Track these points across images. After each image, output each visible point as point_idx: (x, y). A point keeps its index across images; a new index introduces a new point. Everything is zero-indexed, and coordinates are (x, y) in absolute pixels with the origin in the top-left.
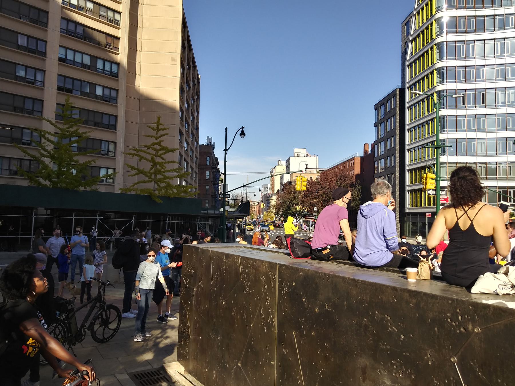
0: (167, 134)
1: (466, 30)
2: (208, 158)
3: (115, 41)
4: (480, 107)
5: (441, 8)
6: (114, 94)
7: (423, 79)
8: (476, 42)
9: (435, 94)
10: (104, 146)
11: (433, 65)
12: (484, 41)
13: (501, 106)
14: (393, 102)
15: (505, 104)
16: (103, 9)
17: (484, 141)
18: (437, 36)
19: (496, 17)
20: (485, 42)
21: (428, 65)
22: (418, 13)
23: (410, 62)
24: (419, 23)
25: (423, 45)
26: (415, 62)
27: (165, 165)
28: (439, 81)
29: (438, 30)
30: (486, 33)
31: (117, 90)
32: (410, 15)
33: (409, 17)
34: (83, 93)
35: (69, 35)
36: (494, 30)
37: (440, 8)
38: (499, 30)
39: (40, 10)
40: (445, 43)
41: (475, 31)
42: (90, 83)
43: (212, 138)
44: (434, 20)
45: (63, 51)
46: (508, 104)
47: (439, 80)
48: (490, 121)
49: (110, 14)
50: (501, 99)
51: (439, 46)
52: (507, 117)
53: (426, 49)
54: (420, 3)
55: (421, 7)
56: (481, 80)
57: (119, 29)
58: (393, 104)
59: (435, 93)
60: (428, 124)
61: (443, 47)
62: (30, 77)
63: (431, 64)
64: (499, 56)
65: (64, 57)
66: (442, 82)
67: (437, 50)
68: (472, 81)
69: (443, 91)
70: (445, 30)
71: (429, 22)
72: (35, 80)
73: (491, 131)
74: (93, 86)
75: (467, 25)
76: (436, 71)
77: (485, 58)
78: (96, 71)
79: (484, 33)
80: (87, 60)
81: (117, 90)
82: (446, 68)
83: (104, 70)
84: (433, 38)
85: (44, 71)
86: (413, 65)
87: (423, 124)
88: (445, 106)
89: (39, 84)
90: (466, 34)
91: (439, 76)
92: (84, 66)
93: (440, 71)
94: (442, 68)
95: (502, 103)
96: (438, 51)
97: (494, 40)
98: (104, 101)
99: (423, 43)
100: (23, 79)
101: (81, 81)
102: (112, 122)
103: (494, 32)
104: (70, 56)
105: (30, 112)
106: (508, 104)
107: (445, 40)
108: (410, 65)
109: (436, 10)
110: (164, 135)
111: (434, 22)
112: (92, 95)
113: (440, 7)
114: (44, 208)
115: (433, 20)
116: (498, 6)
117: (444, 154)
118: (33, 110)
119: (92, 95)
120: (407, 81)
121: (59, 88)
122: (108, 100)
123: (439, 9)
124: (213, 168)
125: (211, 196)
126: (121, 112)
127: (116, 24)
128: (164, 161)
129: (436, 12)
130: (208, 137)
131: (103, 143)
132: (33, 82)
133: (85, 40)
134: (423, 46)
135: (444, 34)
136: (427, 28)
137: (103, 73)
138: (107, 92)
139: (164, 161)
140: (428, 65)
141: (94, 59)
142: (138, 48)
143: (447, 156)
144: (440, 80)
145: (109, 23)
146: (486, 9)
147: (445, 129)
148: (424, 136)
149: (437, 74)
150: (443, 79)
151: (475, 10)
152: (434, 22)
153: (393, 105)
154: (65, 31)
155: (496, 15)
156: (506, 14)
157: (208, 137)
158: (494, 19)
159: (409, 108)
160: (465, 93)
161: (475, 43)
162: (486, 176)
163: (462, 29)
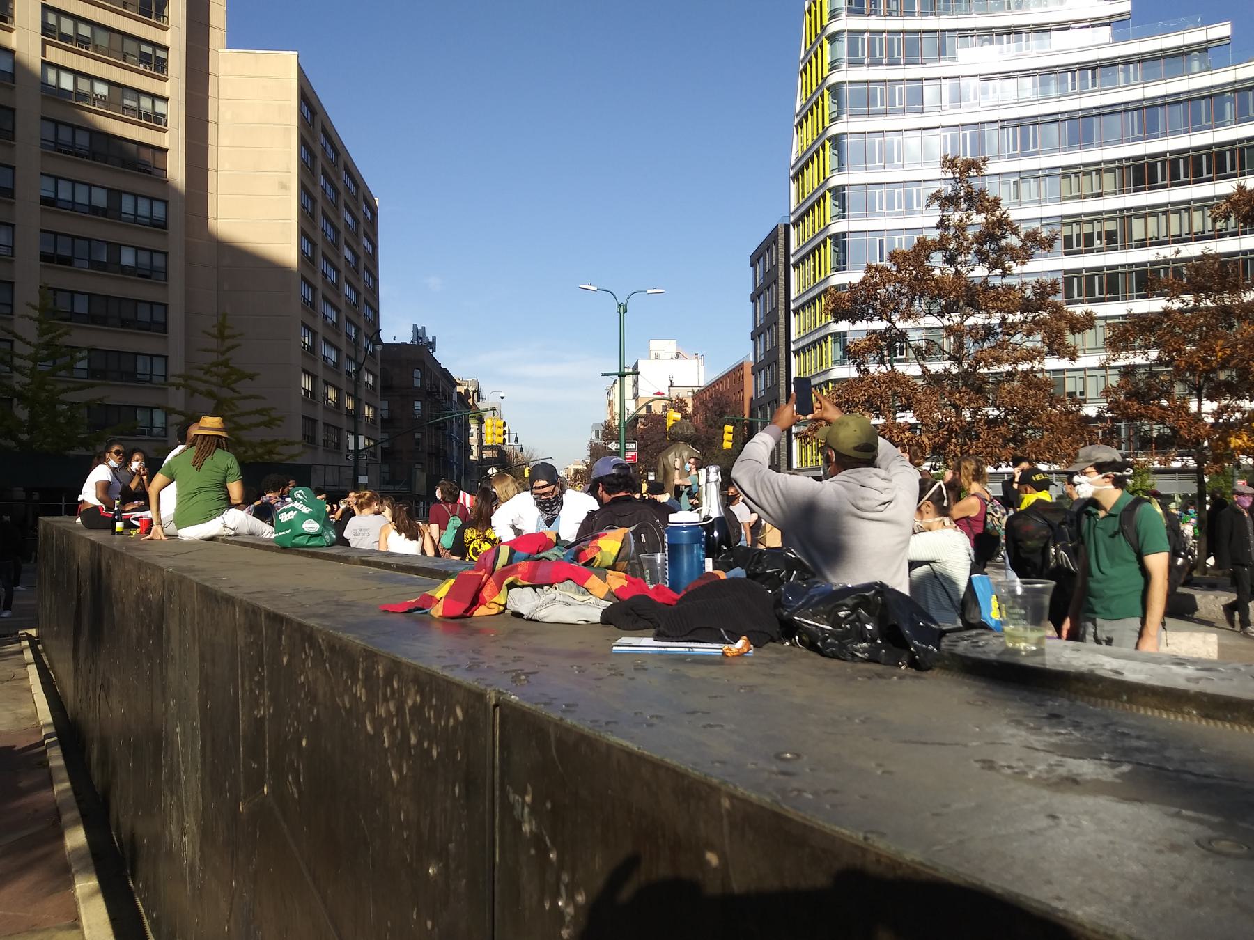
0: (239, 345)
2: (417, 373)
3: (158, 155)
6: (159, 261)
10: (142, 366)
16: (128, 93)
18: (832, 120)
22: (805, 69)
29: (835, 108)
31: (166, 254)
34: (94, 264)
35: (60, 151)
42: (108, 243)
43: (424, 328)
45: (49, 184)
47: (837, 210)
49: (146, 103)
57: (165, 131)
65: (52, 195)
68: (879, 215)
69: (844, 234)
74: (115, 248)
80: (100, 198)
81: (166, 254)
83: (136, 215)
85: (13, 226)
92: (95, 210)
94: (841, 188)
98: (140, 276)
101: (90, 240)
102: (158, 317)
104: (64, 193)
110: (233, 347)
111: (826, 93)
112: (112, 266)
114: (22, 489)
119: (112, 266)
121: (44, 257)
122: (148, 273)
124: (430, 394)
125: (428, 453)
126: (175, 294)
127: (158, 122)
128: (236, 395)
129: (830, 70)
130: (415, 326)
131: (140, 360)
133: (94, 159)
137: (136, 221)
138: (144, 258)
141: (115, 195)
145: (143, 121)
154: (52, 144)
157: (415, 326)
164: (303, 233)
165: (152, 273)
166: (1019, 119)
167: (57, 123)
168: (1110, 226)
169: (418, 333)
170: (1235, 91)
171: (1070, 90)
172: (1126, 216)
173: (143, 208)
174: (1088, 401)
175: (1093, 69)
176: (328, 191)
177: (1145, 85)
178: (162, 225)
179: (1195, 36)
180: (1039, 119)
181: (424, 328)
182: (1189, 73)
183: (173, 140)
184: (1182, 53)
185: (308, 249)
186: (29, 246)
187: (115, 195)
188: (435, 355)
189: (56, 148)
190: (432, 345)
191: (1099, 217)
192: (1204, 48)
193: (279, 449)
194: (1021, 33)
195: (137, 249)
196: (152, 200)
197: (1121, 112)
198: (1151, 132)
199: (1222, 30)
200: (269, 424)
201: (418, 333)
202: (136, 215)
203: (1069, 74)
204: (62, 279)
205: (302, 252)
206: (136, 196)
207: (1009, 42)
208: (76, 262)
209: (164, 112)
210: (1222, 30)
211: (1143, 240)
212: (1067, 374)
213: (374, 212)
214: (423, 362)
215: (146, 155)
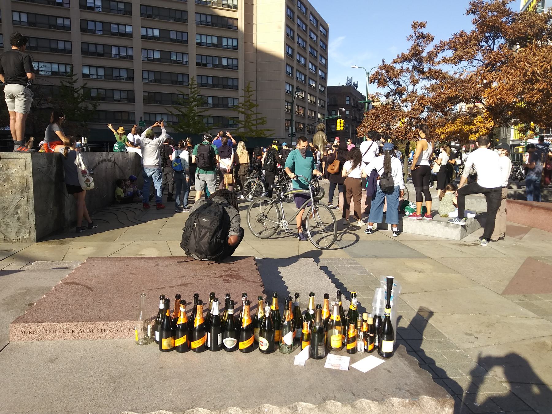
2: (348, 98)
3: (235, 21)
6: (235, 62)
27: (252, 115)
34: (214, 66)
35: (202, 24)
39: (182, 11)
42: (218, 57)
45: (198, 37)
57: (237, 11)
62: (180, 59)
65: (199, 41)
72: (183, 61)
74: (220, 59)
78: (222, 47)
80: (215, 41)
83: (227, 45)
85: (188, 54)
89: (185, 63)
92: (214, 45)
98: (229, 68)
100: (175, 62)
101: (212, 56)
102: (235, 84)
104: (204, 40)
105: (181, 83)
118: (183, 82)
121: (198, 64)
122: (232, 67)
124: (353, 107)
126: (241, 75)
128: (253, 113)
130: (348, 77)
131: (230, 100)
132: (182, 63)
133: (213, 26)
138: (230, 61)
139: (253, 113)
141: (220, 38)
142: (254, 22)
145: (229, 9)
154: (199, 22)
157: (348, 77)
164: (287, 45)
165: (233, 68)
167: (201, 14)
169: (349, 81)
173: (230, 43)
176: (301, 25)
178: (236, 48)
181: (352, 78)
183: (239, 15)
185: (290, 52)
186: (193, 60)
187: (220, 38)
188: (357, 89)
189: (201, 24)
190: (356, 85)
193: (265, 132)
195: (228, 58)
196: (233, 39)
200: (262, 123)
201: (349, 81)
202: (227, 45)
204: (204, 72)
205: (287, 54)
206: (227, 38)
208: (208, 65)
209: (236, 4)
213: (327, 31)
214: (351, 93)
215: (230, 21)
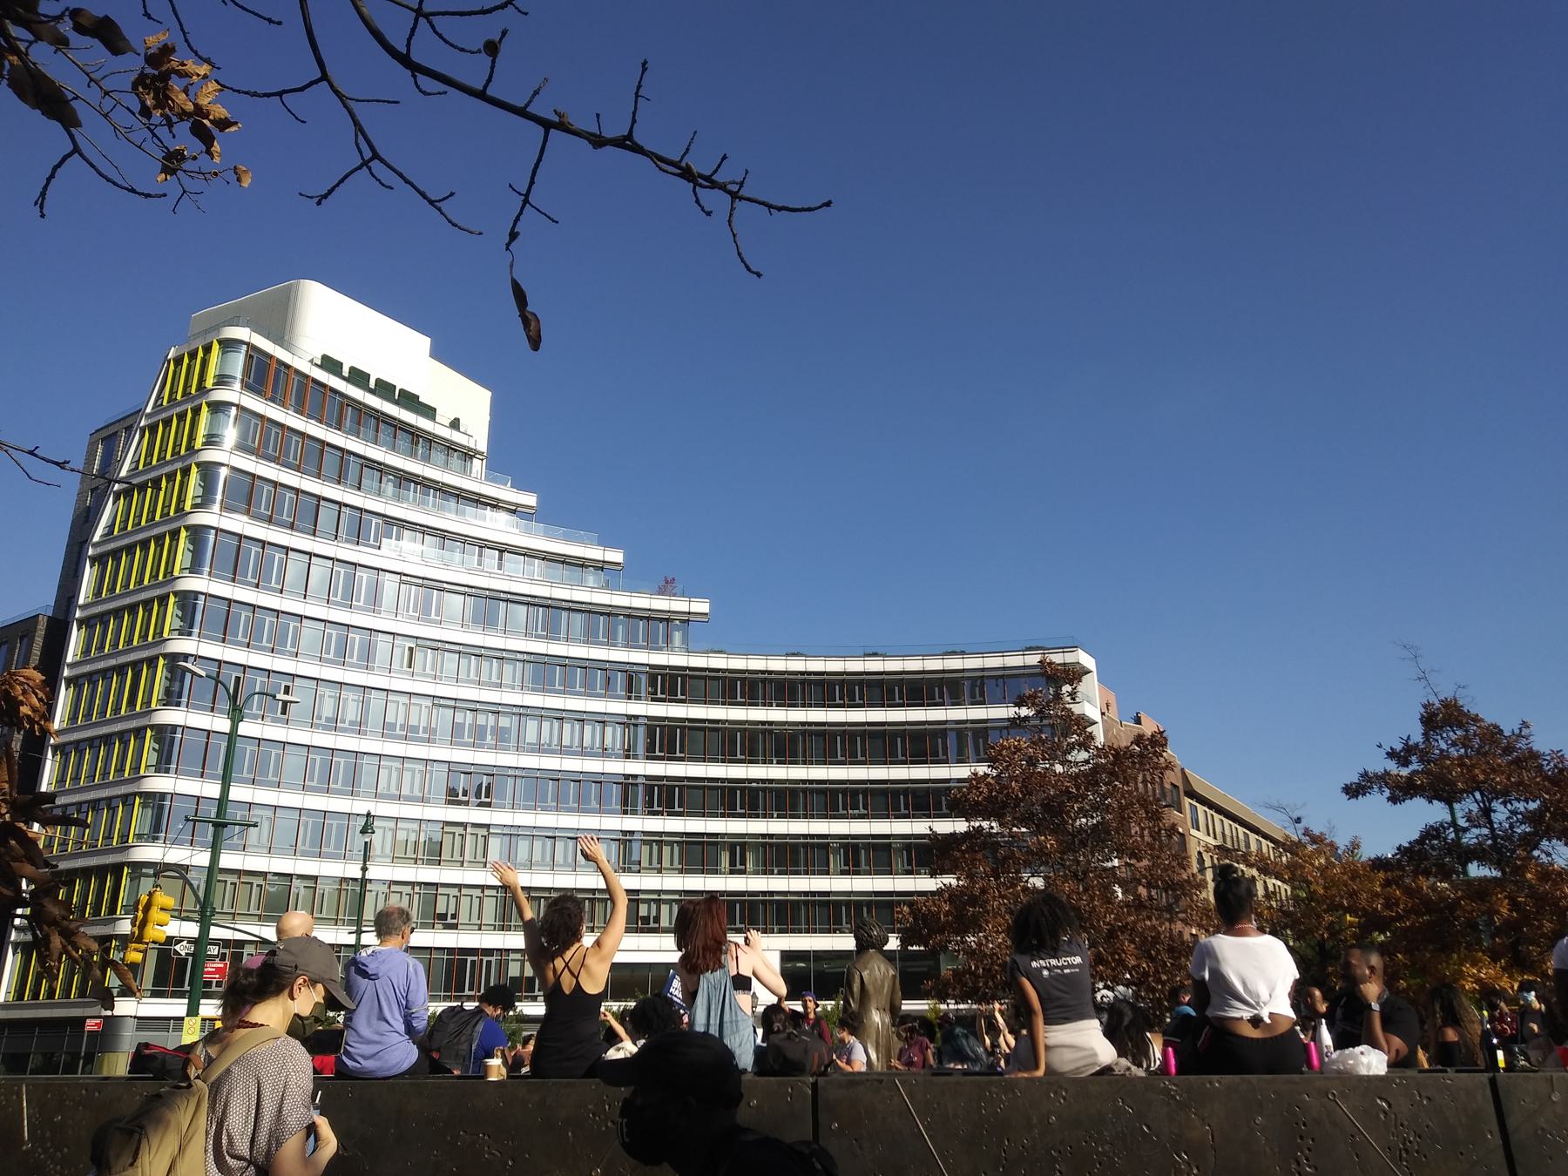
1: (271, 516)
4: (275, 720)
5: (217, 439)
7: (132, 609)
8: (290, 552)
9: (161, 661)
11: (171, 578)
12: (308, 557)
13: (325, 728)
14: (17, 651)
15: (333, 725)
17: (269, 813)
18: (195, 506)
19: (343, 509)
20: (310, 560)
21: (154, 574)
22: (153, 429)
23: (99, 550)
24: (150, 453)
25: (150, 517)
26: (116, 554)
28: (178, 628)
29: (200, 492)
30: (317, 539)
32: (126, 424)
33: (117, 424)
36: (336, 539)
37: (213, 439)
38: (347, 541)
40: (213, 531)
41: (292, 527)
44: (193, 464)
46: (342, 725)
47: (178, 624)
48: (293, 761)
50: (327, 710)
51: (198, 534)
52: (334, 759)
53: (156, 531)
54: (162, 404)
55: (164, 416)
56: (287, 651)
58: (15, 658)
59: (161, 658)
60: (125, 744)
61: (205, 541)
63: (165, 576)
64: (336, 604)
66: (185, 632)
67: (187, 542)
70: (219, 497)
71: (179, 465)
73: (291, 787)
75: (275, 504)
76: (175, 597)
77: (305, 598)
79: (312, 538)
82: (203, 597)
84: (183, 509)
86: (108, 561)
87: (107, 739)
88: (184, 700)
90: (271, 527)
91: (180, 614)
93: (188, 601)
94: (193, 595)
95: (328, 719)
96: (191, 548)
97: (331, 562)
99: (153, 512)
103: (335, 543)
106: (342, 725)
107: (216, 525)
108: (100, 560)
109: (204, 440)
111: (194, 470)
113: (217, 436)
115: (193, 461)
116: (352, 486)
117: (157, 838)
120: (81, 601)
123: (213, 439)
129: (204, 444)
134: (151, 518)
135: (216, 508)
136: (171, 477)
140: (155, 576)
143: (164, 843)
144: (182, 624)
146: (325, 483)
147: (173, 766)
148: (105, 774)
149: (176, 607)
150: (191, 626)
151: (300, 474)
152: (194, 470)
153: (15, 662)
155: (346, 505)
156: (366, 511)
158: (340, 512)
159: (69, 681)
160: (241, 675)
161: (287, 554)
162: (259, 912)
163: (262, 510)
166: (423, 578)
168: (504, 722)
170: (628, 616)
171: (476, 566)
172: (523, 712)
174: (460, 927)
175: (501, 552)
177: (574, 587)
179: (595, 553)
180: (445, 585)
182: (582, 584)
184: (582, 564)
191: (497, 710)
192: (601, 566)
194: (430, 487)
197: (528, 604)
198: (551, 633)
199: (616, 556)
203: (477, 548)
207: (415, 492)
210: (616, 556)
211: (534, 744)
212: (441, 890)
